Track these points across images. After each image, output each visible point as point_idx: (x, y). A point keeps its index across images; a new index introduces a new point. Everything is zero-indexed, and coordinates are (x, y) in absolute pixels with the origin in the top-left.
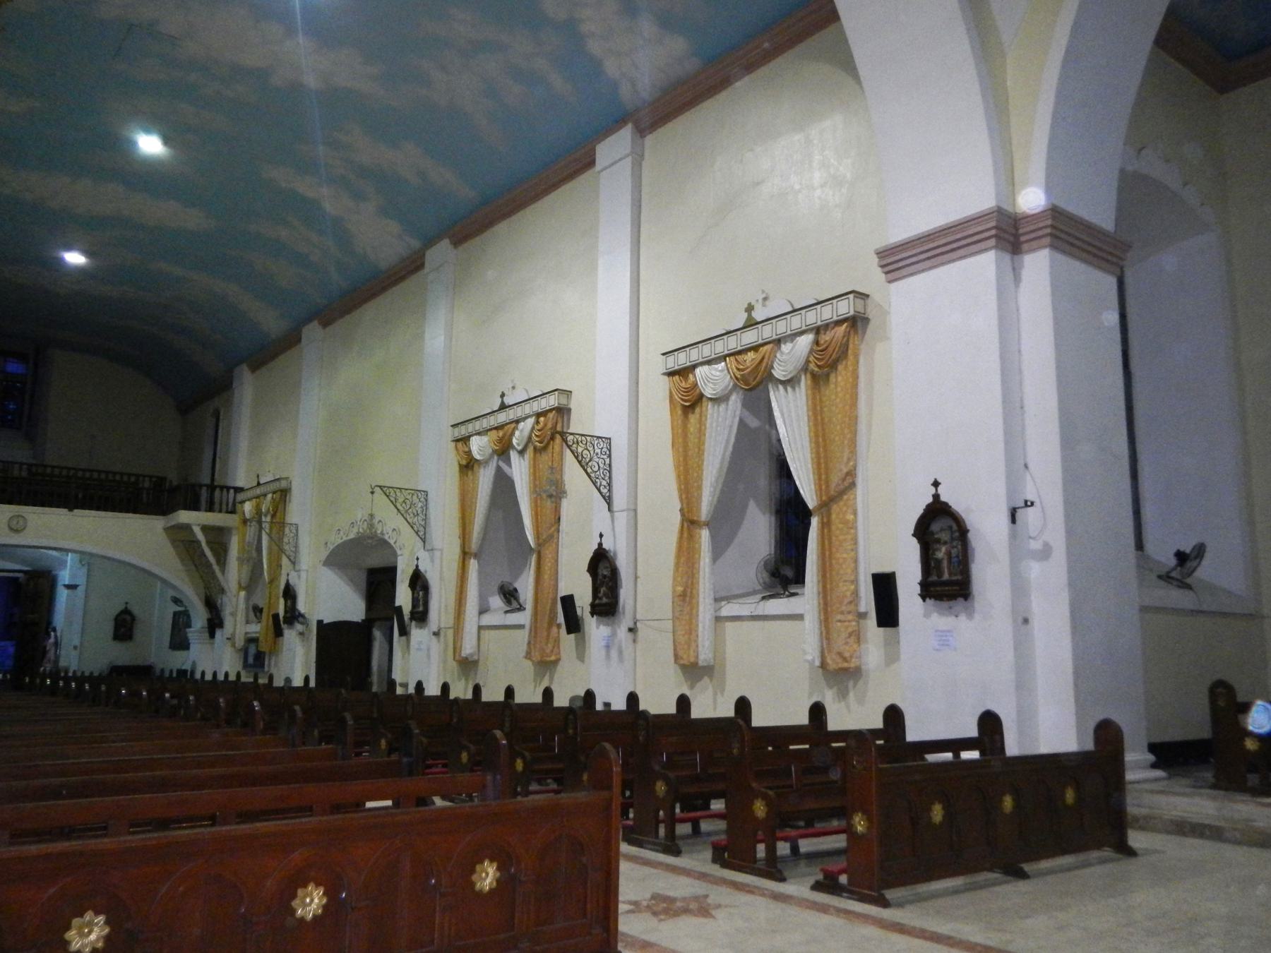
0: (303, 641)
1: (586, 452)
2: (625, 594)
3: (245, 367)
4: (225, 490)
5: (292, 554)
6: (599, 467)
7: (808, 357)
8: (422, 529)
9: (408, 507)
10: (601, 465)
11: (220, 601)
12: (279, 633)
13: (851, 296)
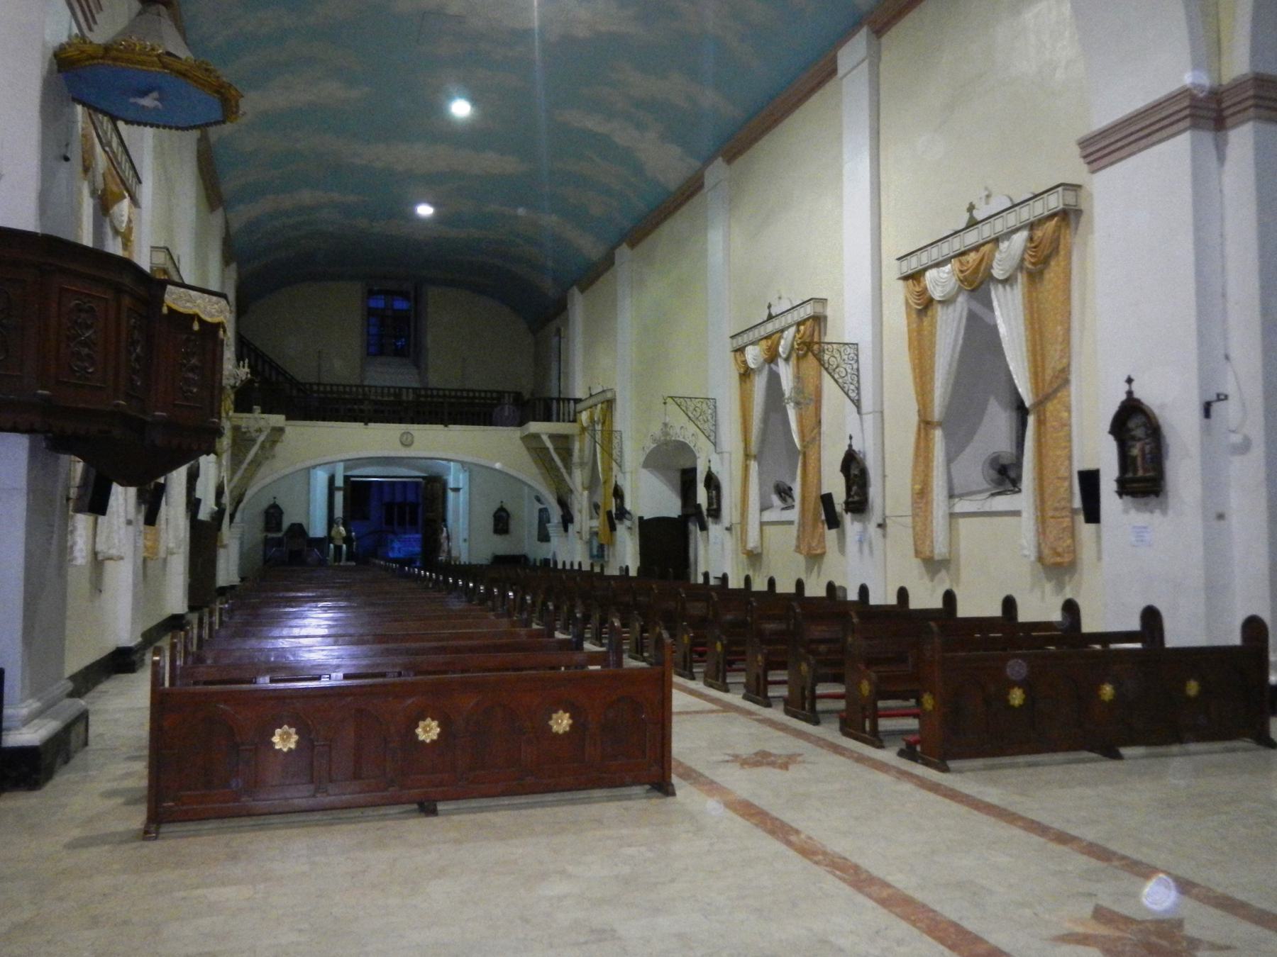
0: (631, 534)
1: (833, 359)
2: (874, 492)
3: (575, 290)
4: (566, 402)
5: (617, 458)
6: (847, 372)
7: (1023, 254)
8: (712, 434)
9: (699, 414)
10: (849, 371)
11: (569, 500)
12: (613, 528)
13: (1060, 189)
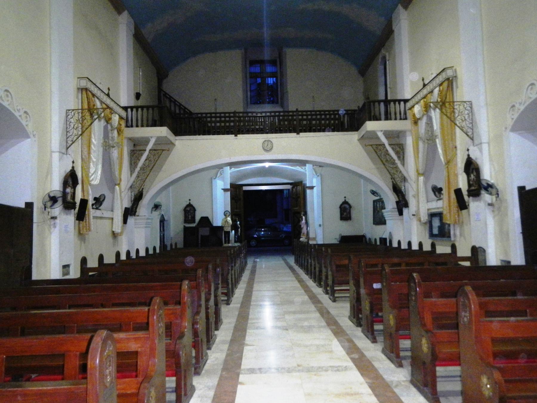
4: (397, 103)
12: (462, 205)
